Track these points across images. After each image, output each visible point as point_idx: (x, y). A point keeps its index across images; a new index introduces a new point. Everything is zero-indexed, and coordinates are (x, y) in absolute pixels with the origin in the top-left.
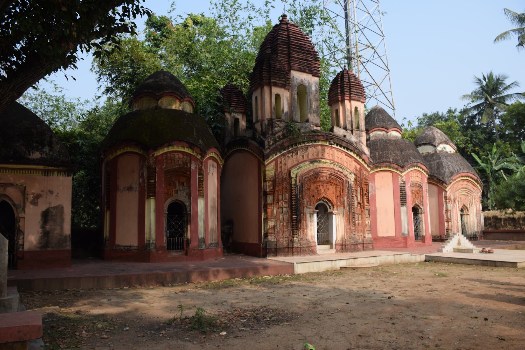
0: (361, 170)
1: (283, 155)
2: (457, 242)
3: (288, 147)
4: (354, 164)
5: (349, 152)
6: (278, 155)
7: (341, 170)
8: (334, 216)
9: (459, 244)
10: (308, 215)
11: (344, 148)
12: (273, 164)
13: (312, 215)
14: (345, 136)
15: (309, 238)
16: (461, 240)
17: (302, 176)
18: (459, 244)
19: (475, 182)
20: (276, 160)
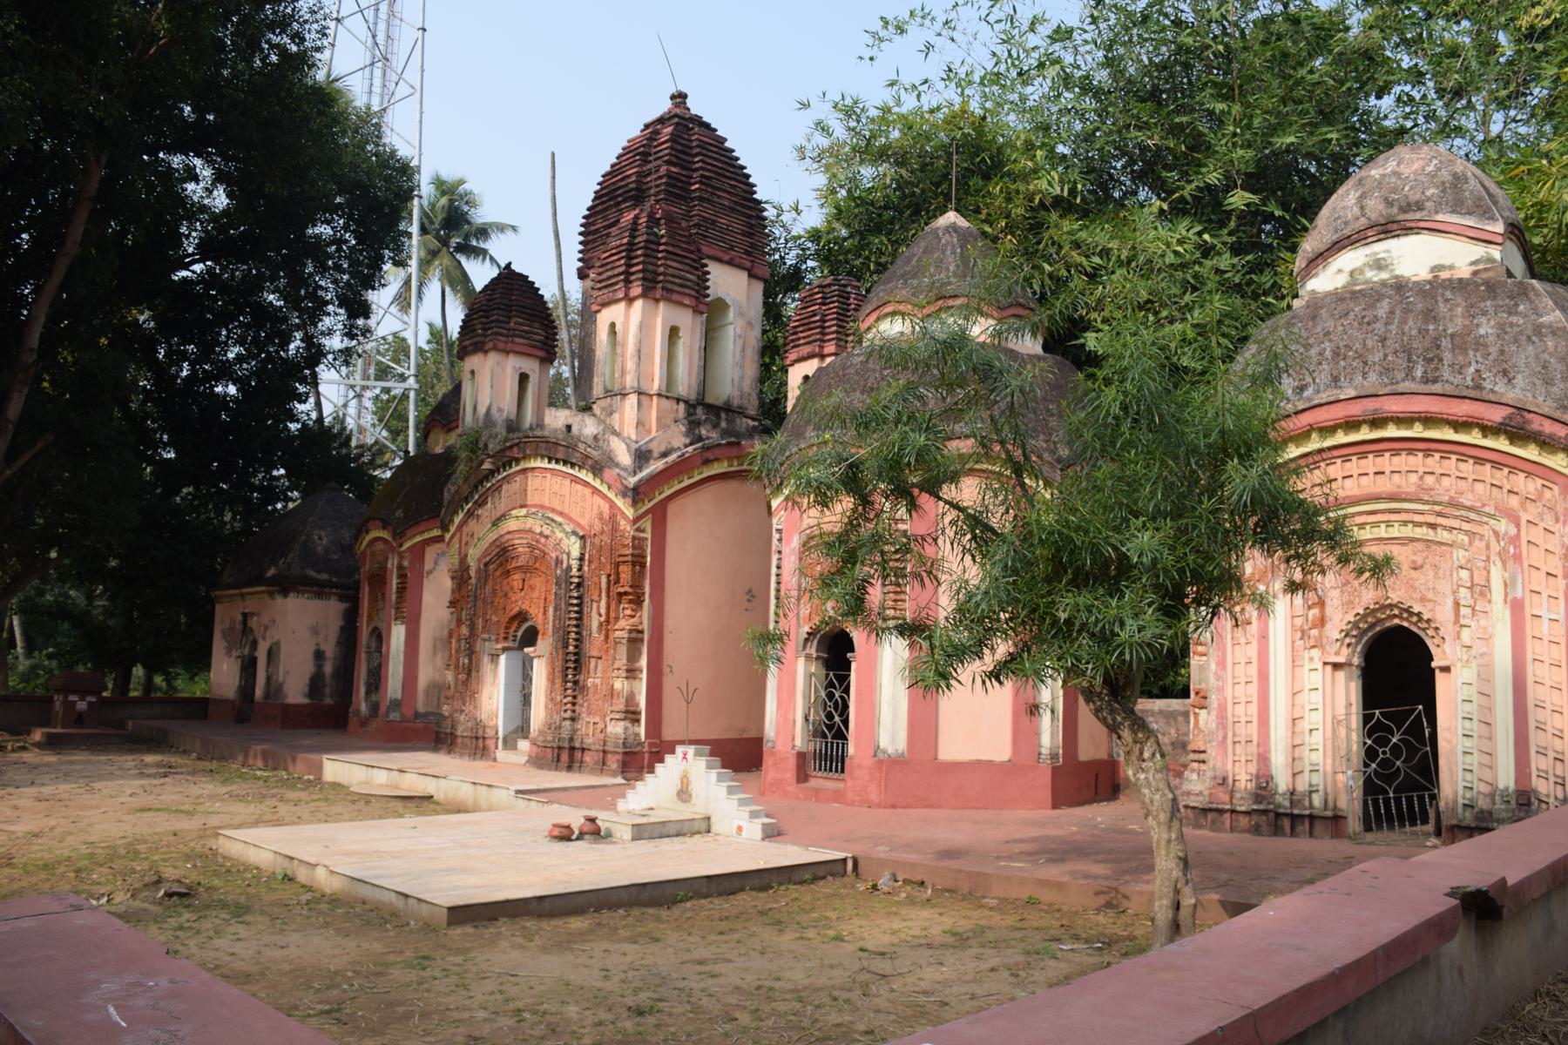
0: (613, 517)
1: (470, 514)
2: (675, 785)
3: (471, 494)
4: (598, 500)
5: (575, 472)
6: (461, 515)
7: (547, 532)
8: (535, 662)
9: (684, 794)
10: (486, 659)
11: (565, 462)
12: (456, 539)
13: (494, 657)
14: (569, 427)
15: (483, 714)
16: (693, 778)
17: (479, 560)
18: (684, 794)
19: (1502, 444)
20: (460, 528)
